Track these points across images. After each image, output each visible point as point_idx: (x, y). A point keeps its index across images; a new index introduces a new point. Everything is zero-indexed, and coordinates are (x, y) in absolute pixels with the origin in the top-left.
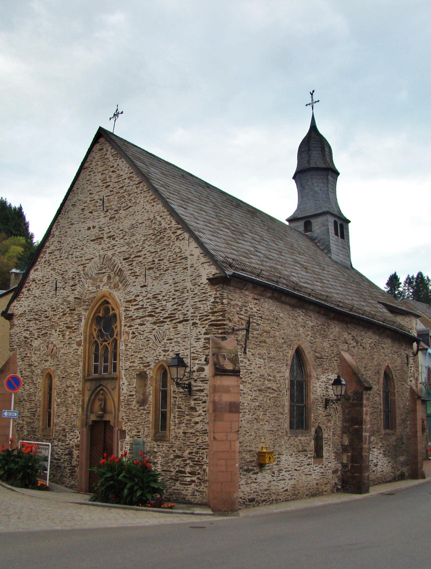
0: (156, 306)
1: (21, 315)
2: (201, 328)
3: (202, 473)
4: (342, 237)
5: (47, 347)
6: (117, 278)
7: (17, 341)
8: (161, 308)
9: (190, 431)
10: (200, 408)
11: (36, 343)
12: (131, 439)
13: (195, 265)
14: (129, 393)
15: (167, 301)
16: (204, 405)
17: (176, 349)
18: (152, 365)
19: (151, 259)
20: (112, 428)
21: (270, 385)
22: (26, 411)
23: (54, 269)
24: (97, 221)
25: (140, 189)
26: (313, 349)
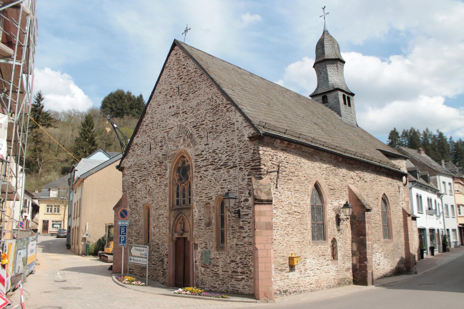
0: (215, 158)
2: (245, 172)
3: (249, 273)
4: (350, 105)
5: (146, 188)
7: (127, 185)
8: (218, 159)
9: (240, 243)
10: (247, 227)
11: (139, 186)
12: (202, 250)
13: (240, 128)
14: (199, 218)
15: (222, 154)
16: (249, 225)
17: (229, 187)
18: (214, 199)
19: (210, 126)
20: (189, 242)
21: (296, 210)
22: (134, 232)
23: (149, 136)
24: (175, 102)
25: (202, 78)
26: (328, 183)
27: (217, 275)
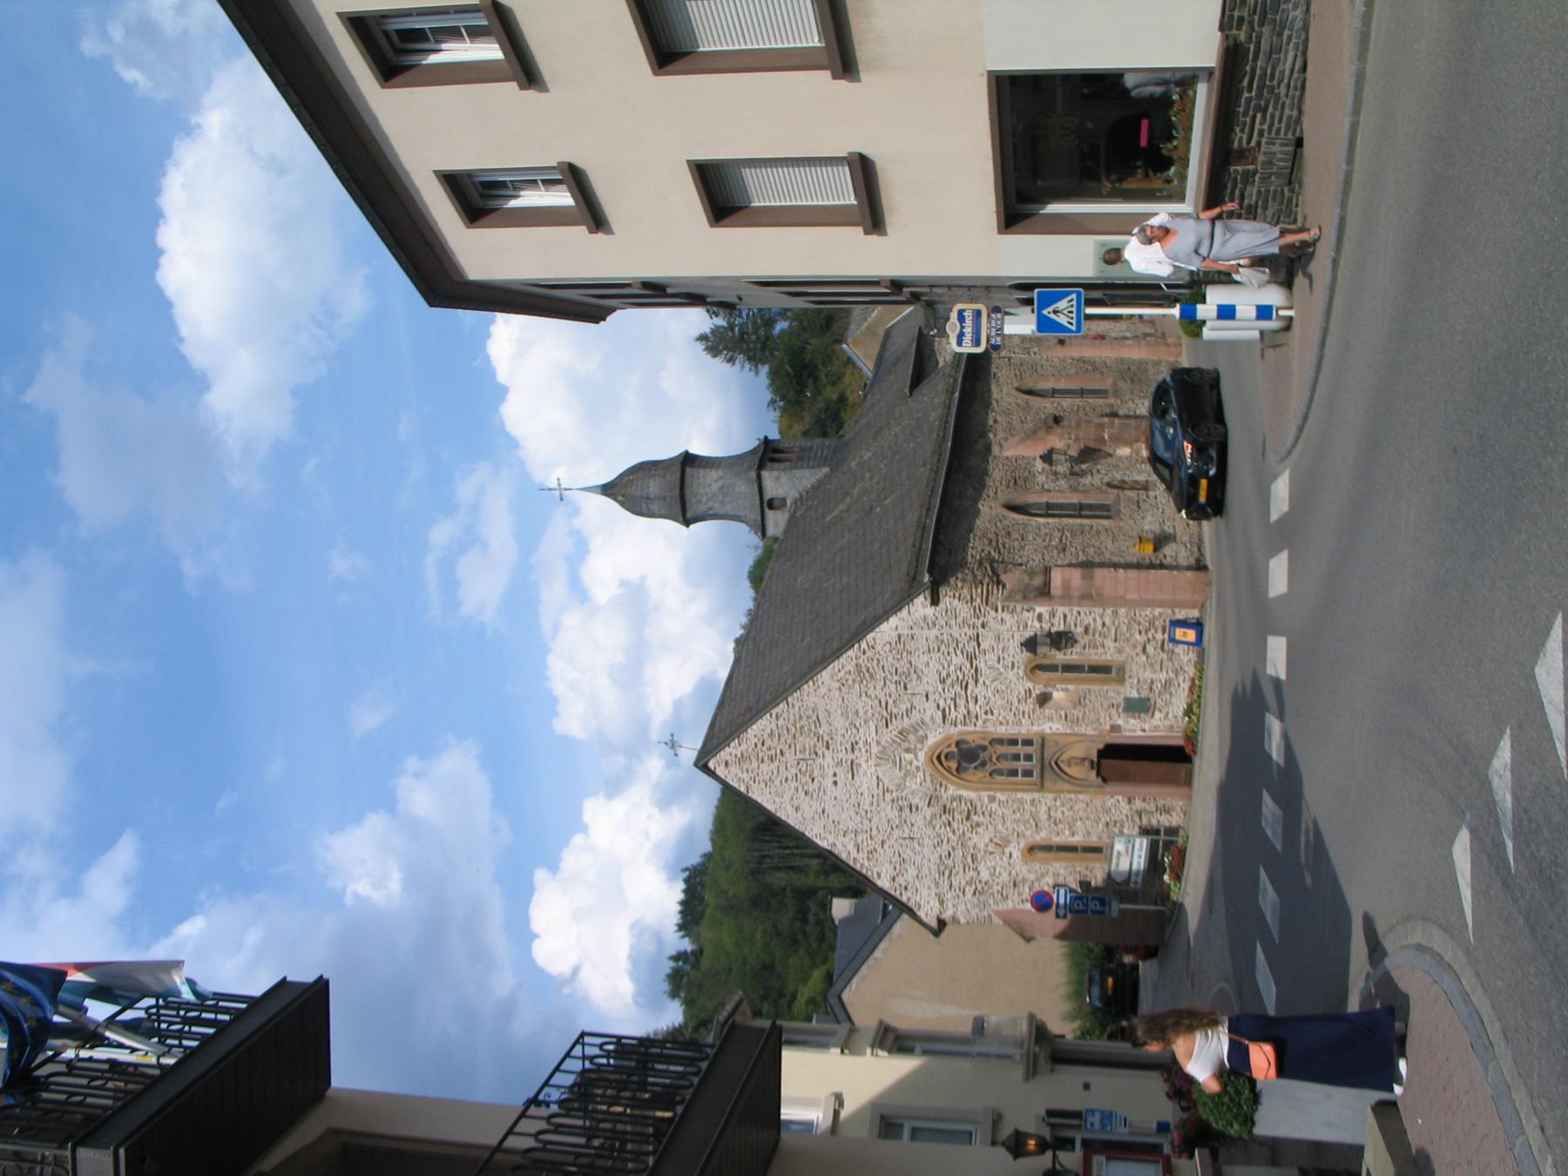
1: (942, 903)
6: (911, 737)
11: (985, 875)
19: (893, 687)
23: (883, 843)
27: (1167, 684)
